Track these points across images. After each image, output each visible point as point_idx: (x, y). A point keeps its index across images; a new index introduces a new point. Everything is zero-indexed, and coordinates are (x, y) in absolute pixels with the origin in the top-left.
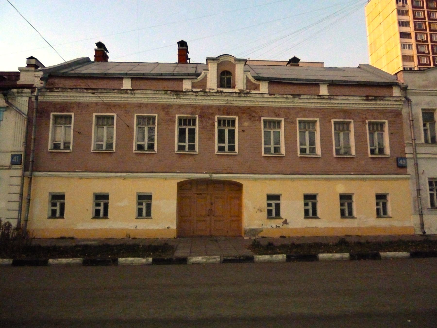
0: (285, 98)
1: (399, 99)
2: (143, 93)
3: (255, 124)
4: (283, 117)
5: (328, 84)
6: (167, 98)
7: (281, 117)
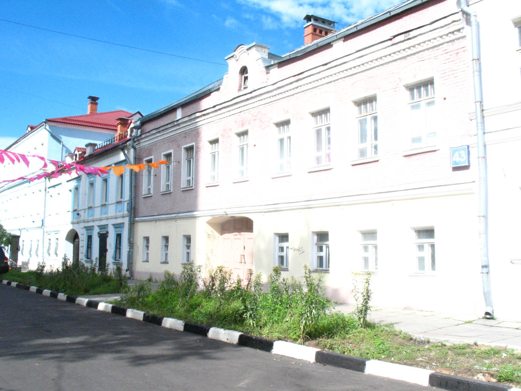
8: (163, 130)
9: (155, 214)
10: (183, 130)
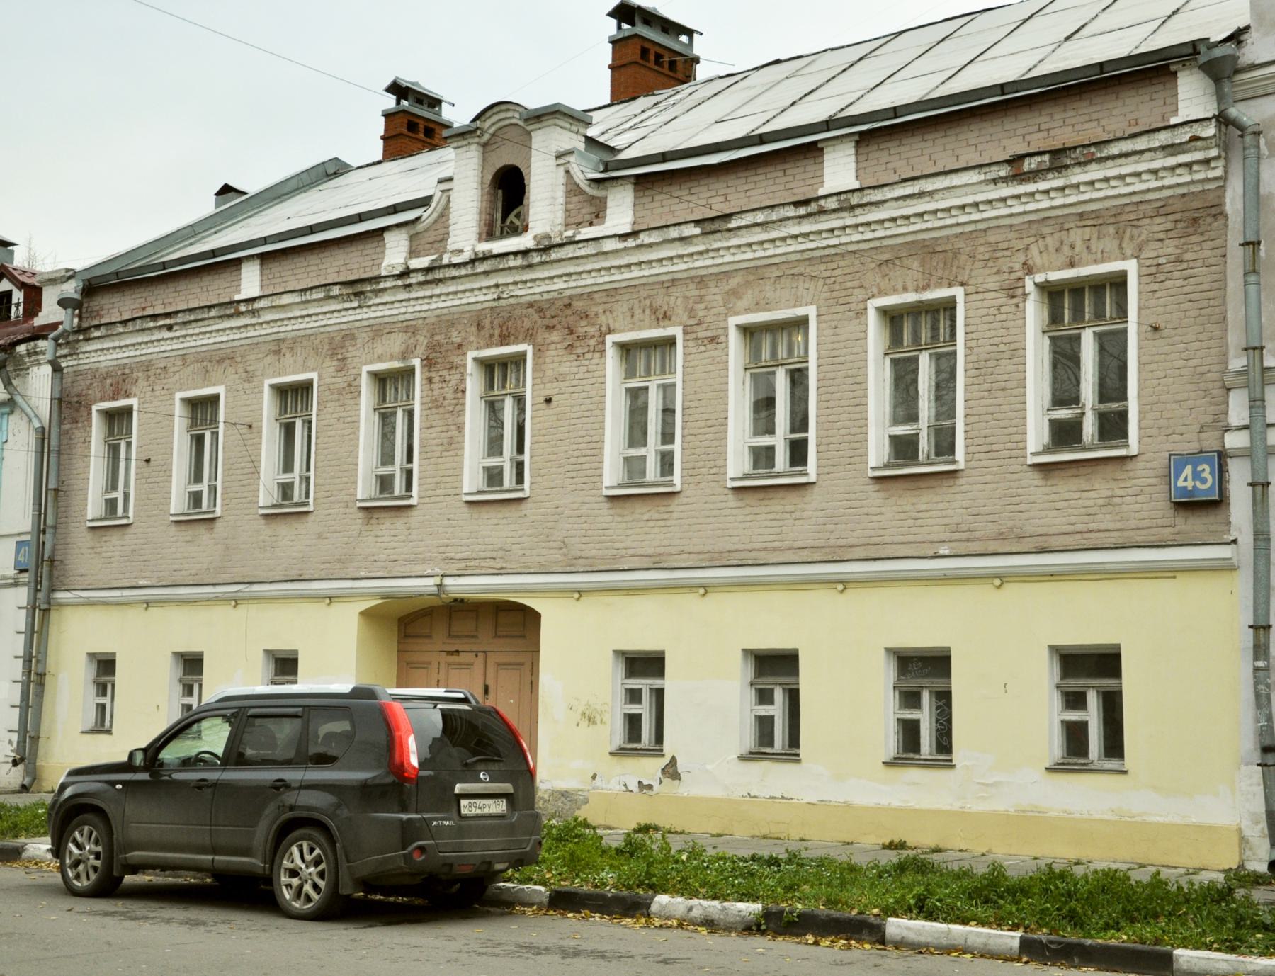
1: (1187, 138)
3: (585, 369)
5: (857, 138)
7: (673, 325)
8: (185, 323)
9: (142, 582)
10: (269, 331)
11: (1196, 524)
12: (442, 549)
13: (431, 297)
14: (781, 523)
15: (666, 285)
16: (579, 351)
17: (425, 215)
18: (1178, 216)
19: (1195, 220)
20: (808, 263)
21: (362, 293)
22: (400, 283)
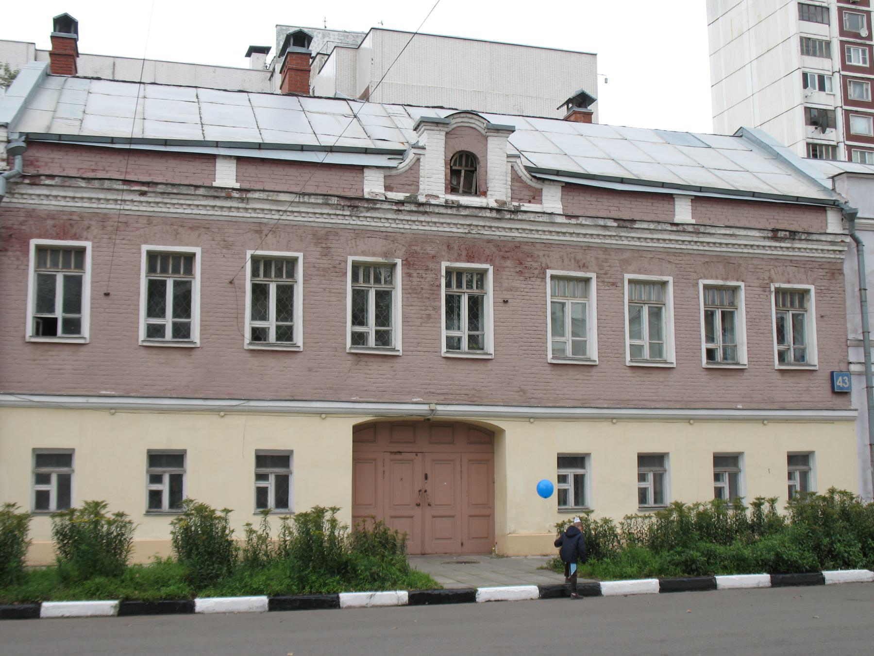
0: (600, 227)
1: (840, 240)
2: (270, 198)
3: (531, 287)
4: (594, 272)
6: (328, 214)
11: (839, 401)
12: (426, 386)
13: (414, 221)
14: (657, 387)
15: (584, 248)
16: (527, 275)
17: (401, 166)
18: (827, 270)
19: (833, 274)
20: (667, 254)
21: (357, 207)
22: (395, 208)
